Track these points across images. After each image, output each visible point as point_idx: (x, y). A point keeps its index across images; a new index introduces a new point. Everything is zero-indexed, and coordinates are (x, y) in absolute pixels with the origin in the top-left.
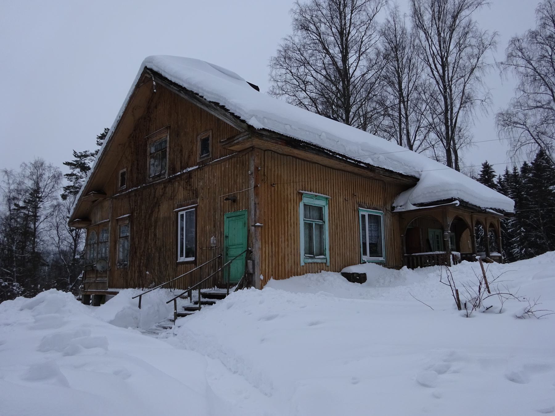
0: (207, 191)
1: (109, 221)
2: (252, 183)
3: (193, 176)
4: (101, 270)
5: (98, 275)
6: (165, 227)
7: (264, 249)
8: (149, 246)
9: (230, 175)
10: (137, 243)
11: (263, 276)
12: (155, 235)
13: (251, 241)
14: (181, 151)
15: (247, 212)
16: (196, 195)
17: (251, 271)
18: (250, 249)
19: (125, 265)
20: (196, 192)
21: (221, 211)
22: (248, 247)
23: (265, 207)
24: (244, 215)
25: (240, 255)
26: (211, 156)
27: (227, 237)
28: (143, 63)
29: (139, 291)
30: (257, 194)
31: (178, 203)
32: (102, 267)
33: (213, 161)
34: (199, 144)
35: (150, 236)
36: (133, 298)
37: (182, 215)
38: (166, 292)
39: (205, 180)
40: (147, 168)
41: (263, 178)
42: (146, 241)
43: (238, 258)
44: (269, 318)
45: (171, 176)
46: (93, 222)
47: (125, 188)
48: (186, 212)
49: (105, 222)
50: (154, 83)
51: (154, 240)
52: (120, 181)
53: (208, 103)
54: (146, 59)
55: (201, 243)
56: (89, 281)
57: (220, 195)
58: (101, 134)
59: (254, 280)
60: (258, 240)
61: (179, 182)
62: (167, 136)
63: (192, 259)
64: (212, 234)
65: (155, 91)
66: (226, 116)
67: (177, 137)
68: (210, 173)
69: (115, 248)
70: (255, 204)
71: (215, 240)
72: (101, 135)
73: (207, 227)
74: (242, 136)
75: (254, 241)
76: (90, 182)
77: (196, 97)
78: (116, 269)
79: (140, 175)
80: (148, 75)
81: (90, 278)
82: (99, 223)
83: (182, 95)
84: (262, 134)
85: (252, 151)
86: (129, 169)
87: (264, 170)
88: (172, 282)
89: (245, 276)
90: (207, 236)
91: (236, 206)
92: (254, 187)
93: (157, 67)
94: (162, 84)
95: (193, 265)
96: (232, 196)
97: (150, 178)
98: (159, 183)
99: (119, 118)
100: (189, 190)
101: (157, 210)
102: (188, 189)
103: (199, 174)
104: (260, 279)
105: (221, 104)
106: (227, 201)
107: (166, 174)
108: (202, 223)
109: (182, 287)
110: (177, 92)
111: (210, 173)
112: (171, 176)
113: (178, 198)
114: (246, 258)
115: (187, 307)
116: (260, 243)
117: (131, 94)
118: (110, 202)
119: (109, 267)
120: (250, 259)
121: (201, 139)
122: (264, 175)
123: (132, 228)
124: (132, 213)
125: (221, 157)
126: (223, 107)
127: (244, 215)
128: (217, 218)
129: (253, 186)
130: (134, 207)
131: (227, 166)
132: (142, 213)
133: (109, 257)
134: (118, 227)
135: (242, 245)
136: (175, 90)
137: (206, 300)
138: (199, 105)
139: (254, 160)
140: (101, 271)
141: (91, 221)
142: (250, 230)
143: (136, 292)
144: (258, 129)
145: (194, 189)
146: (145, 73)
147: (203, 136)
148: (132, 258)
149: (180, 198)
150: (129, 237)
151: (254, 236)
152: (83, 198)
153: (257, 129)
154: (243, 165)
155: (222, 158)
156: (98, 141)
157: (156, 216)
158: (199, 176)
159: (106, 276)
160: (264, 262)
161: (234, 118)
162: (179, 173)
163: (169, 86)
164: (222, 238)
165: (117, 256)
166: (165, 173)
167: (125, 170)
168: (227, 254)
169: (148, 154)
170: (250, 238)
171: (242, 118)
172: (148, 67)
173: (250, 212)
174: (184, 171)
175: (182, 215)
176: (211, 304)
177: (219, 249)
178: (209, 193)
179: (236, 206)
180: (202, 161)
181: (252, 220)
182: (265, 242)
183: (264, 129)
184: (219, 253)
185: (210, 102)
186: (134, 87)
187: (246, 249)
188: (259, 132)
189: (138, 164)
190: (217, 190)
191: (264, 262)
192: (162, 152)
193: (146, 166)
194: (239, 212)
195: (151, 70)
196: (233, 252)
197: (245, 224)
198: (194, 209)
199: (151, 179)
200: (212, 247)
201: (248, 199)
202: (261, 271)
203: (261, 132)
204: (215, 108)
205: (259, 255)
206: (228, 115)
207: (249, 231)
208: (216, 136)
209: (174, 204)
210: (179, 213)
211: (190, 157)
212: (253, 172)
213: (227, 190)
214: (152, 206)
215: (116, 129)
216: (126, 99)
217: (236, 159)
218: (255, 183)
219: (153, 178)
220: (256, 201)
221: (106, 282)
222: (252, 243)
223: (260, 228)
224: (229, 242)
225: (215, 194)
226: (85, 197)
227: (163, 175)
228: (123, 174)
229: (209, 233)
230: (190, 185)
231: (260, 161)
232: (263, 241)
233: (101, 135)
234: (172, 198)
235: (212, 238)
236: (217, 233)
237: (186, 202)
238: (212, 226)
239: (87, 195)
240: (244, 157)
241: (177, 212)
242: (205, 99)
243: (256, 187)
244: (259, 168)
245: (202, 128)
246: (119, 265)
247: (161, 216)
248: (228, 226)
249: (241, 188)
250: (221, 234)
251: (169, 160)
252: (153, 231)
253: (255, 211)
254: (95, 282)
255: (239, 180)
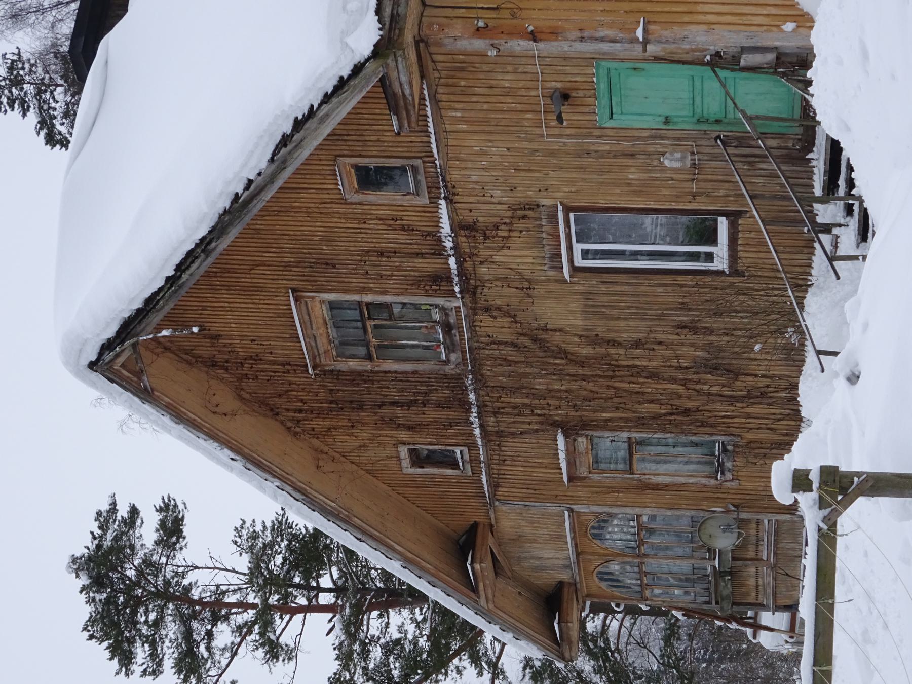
0: (522, 174)
1: (571, 510)
2: (521, 45)
3: (469, 218)
4: (735, 535)
5: (751, 554)
6: (615, 312)
7: (711, 18)
8: (670, 366)
9: (485, 107)
10: (654, 408)
11: (786, 22)
12: (637, 344)
13: (687, 53)
14: (381, 254)
15: (603, 63)
16: (530, 209)
17: (770, 57)
18: (708, 58)
19: (724, 450)
20: (521, 209)
21: (590, 136)
22: (703, 64)
23: (590, 11)
24: (609, 70)
25: (724, 86)
26: (418, 162)
27: (667, 121)
28: (78, 374)
29: (811, 357)
30: (555, 34)
31: (546, 268)
32: (724, 532)
33: (432, 156)
34: (371, 196)
35: (638, 363)
36: (823, 371)
37: (585, 254)
38: (814, 294)
39: (487, 179)
40: (415, 372)
41: (506, 14)
42: (654, 375)
43: (731, 92)
44: (865, 55)
45: (457, 289)
46: (565, 576)
47: (465, 449)
48: (577, 242)
49: (573, 529)
50: (165, 333)
51: (653, 349)
52: (441, 470)
53: (273, 166)
54: (66, 364)
55: (677, 196)
56: (769, 591)
57: (542, 136)
58: (111, 659)
59: (796, 50)
60: (686, 33)
61: (482, 263)
62: (322, 302)
63: (723, 224)
64: (655, 163)
65: (195, 330)
66: (327, 115)
67: (334, 267)
68: (469, 165)
69: (665, 487)
70: (582, 39)
71: (672, 154)
72: (116, 660)
73: (631, 177)
74: (395, 74)
75: (688, 47)
76: (433, 575)
77: (244, 201)
78: (734, 484)
79: (434, 397)
80: (121, 360)
81: (757, 586)
82: (571, 552)
83: (223, 244)
84: (392, 15)
85: (427, 45)
86: (404, 435)
87: (483, 8)
88: (785, 273)
89: (783, 75)
90: (657, 179)
91: (581, 93)
92: (535, 41)
93: (108, 324)
94: (167, 308)
95: (740, 222)
96: (549, 101)
97: (448, 362)
98: (472, 328)
99: (239, 465)
100: (510, 230)
101: (557, 338)
102: (505, 234)
103: (466, 199)
104: (794, 31)
105: (288, 128)
106: (564, 116)
107: (448, 305)
108: (618, 191)
109: (805, 257)
110: (210, 260)
111: (469, 165)
112: (457, 289)
113: (531, 267)
114: (732, 70)
115: (859, 234)
116: (693, 28)
117: (167, 420)
118: (505, 508)
119: (727, 511)
120: (736, 59)
121: (357, 192)
122: (496, 8)
123: (606, 425)
124: (556, 425)
125: (427, 131)
126: (298, 124)
127: (609, 70)
128: (607, 148)
129: (531, 42)
130: (535, 419)
131: (459, 114)
132: (559, 391)
133: (693, 513)
134: (595, 477)
135: (695, 79)
136: (198, 268)
137: (842, 182)
138: (268, 195)
139: (455, 38)
140: (740, 535)
141: (561, 584)
142: (655, 57)
143: (808, 372)
144: (380, 29)
145: (509, 214)
146: (111, 367)
147: (347, 184)
148: (702, 426)
149: (530, 260)
150: (634, 435)
151: (673, 46)
152: (483, 602)
153: (381, 33)
154: (462, 70)
155: (431, 130)
156: (144, 673)
157: (576, 339)
158: (471, 199)
159: (754, 526)
160: (746, 20)
161: (341, 92)
162: (452, 262)
163: (180, 287)
164: (670, 134)
165: (691, 480)
166: (443, 309)
167: (404, 451)
168: (718, 121)
169: (369, 368)
170: (676, 57)
171: (346, 73)
172: (93, 358)
173: (604, 54)
174: (449, 244)
175: (585, 254)
176: (850, 169)
177: (699, 143)
178: (529, 171)
179: (581, 93)
180: (428, 188)
181: (625, 50)
182: (691, 13)
183: (378, 12)
184: (713, 142)
185: (272, 160)
186: (147, 407)
187: (708, 68)
188: (387, 26)
189: (394, 403)
190: (525, 145)
191: (746, 20)
192: (370, 318)
193: (406, 373)
194: (598, 83)
195: (107, 346)
196: (713, 105)
197: (635, 69)
198: (572, 216)
199: (453, 357)
200: (694, 165)
201: (565, 59)
202: (774, 29)
203: (387, 20)
204: (296, 146)
205: (725, 34)
206: (325, 108)
207: (657, 59)
208: (360, 144)
209: (548, 281)
210: (576, 264)
211: (409, 226)
212: (492, 42)
213: (529, 116)
214: (541, 354)
215: (275, 476)
216: (180, 438)
217: (440, 90)
218: (522, 37)
219: (450, 349)
220: (573, 38)
221: (777, 521)
222: (693, 50)
223: (652, 27)
224: (684, 113)
225: (537, 151)
226: (482, 593)
227: (447, 315)
228: (418, 459)
229: (650, 171)
230: (496, 227)
231: (455, 20)
232: (686, 18)
233: (116, 660)
234: (527, 286)
235: (667, 163)
236: (651, 149)
237: (545, 242)
238: (630, 162)
239: (475, 590)
240: (440, 66)
241: (575, 270)
242: (259, 174)
243: (534, 37)
244: (481, 24)
245: (325, 187)
246: (723, 473)
247: (577, 322)
248: (635, 117)
249: (529, 77)
250: (656, 136)
251: (402, 294)
252: (622, 351)
253: (602, 40)
254: (774, 567)
255: (506, 80)
